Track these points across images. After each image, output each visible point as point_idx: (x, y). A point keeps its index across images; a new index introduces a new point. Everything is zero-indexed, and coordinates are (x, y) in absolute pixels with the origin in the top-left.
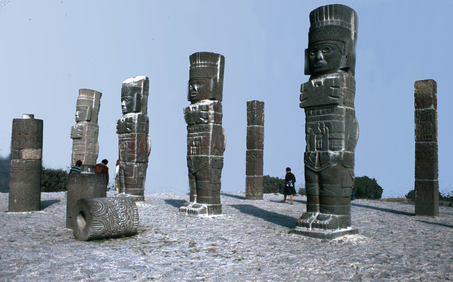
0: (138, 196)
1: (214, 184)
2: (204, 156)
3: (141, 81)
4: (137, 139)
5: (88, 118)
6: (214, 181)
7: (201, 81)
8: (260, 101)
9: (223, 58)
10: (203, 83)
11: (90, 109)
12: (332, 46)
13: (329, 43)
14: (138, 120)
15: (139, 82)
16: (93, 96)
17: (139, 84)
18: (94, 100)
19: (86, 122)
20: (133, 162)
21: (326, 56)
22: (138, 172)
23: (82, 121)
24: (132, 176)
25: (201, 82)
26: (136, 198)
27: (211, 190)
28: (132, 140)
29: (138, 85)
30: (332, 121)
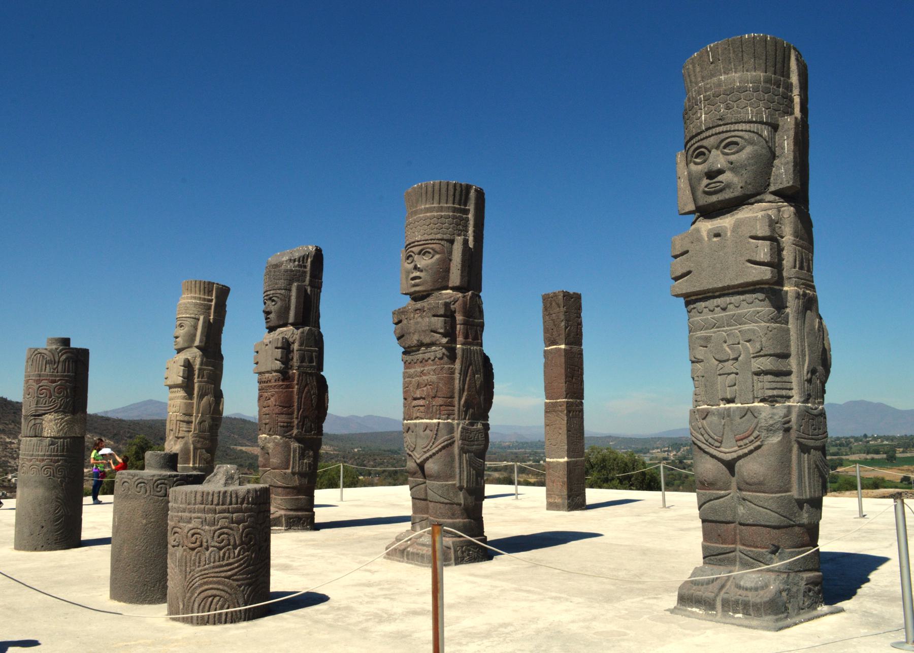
0: (300, 513)
3: (304, 258)
4: (297, 384)
5: (200, 342)
8: (571, 291)
9: (480, 194)
10: (436, 252)
11: (204, 322)
12: (746, 135)
13: (738, 130)
16: (212, 296)
18: (213, 303)
19: (196, 350)
21: (732, 163)
22: (300, 460)
24: (288, 468)
25: (430, 250)
27: (460, 504)
28: (288, 387)
29: (299, 266)
30: (757, 326)
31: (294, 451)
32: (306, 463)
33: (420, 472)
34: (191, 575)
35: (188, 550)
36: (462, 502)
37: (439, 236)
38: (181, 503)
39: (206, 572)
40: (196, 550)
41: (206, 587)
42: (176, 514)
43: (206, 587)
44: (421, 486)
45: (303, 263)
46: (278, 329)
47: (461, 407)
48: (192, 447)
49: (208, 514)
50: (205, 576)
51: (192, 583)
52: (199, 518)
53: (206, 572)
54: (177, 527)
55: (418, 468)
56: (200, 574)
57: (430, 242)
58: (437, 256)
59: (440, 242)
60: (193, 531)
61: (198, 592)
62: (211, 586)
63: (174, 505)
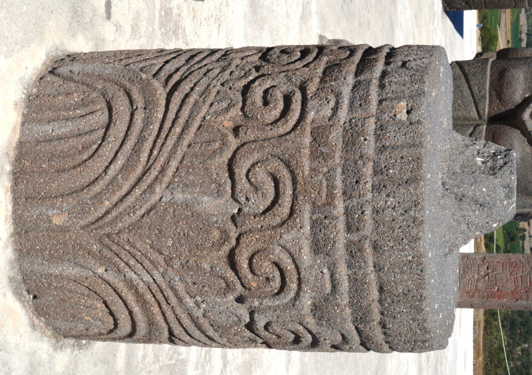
33: (503, 110)
34: (155, 256)
35: (226, 248)
38: (376, 211)
39: (173, 300)
40: (230, 274)
41: (131, 299)
42: (338, 192)
43: (131, 299)
44: (474, 109)
49: (351, 304)
50: (160, 296)
51: (132, 262)
52: (334, 287)
53: (173, 300)
54: (295, 197)
55: (510, 106)
56: (164, 286)
60: (291, 267)
61: (110, 276)
62: (136, 309)
63: (368, 170)
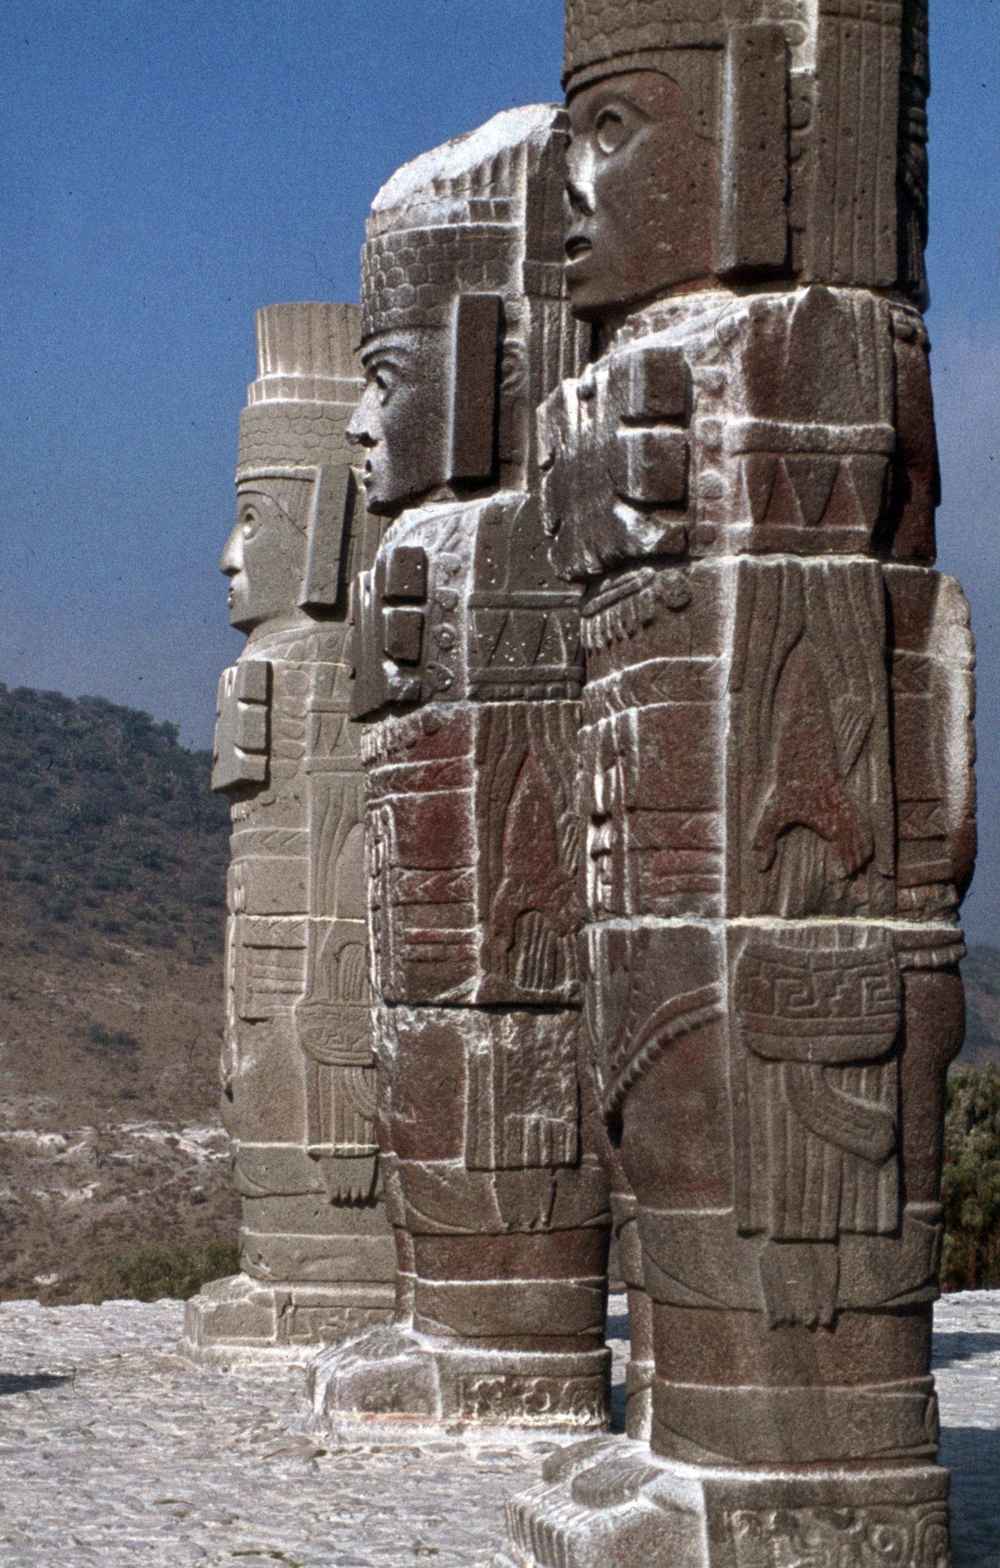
0: (515, 1356)
1: (779, 1240)
2: (664, 923)
6: (782, 1206)
7: (619, 98)
10: (643, 115)
14: (485, 575)
15: (487, 178)
17: (485, 196)
19: (308, 623)
20: (456, 1004)
22: (502, 1108)
23: (276, 615)
24: (452, 1153)
26: (493, 1372)
28: (433, 778)
29: (478, 210)
31: (474, 1072)
32: (536, 1127)
36: (762, 1303)
37: (647, 36)
45: (494, 192)
46: (407, 514)
47: (748, 855)
48: (300, 1062)
57: (617, 65)
58: (645, 133)
59: (656, 60)
